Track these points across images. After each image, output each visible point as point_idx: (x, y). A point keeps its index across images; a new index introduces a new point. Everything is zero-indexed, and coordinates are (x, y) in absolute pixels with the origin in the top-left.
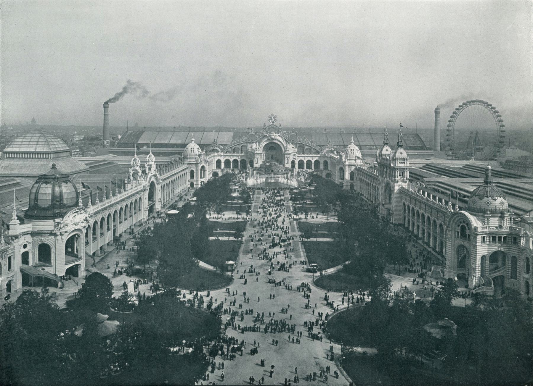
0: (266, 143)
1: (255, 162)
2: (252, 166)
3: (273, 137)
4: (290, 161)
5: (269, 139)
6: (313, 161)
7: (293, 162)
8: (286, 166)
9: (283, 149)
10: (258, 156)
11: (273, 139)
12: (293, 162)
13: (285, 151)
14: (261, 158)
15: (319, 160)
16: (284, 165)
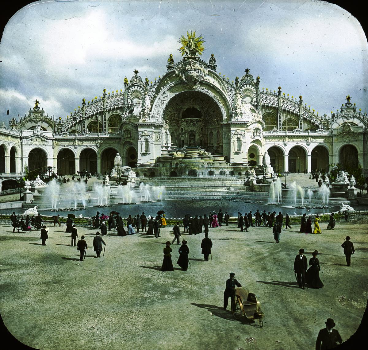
0: (170, 95)
1: (141, 148)
2: (131, 159)
3: (194, 74)
4: (247, 145)
5: (182, 83)
6: (309, 149)
7: (253, 153)
8: (235, 159)
9: (223, 111)
10: (147, 131)
11: (193, 81)
12: (253, 153)
13: (230, 116)
14: (158, 139)
15: (327, 146)
16: (227, 159)
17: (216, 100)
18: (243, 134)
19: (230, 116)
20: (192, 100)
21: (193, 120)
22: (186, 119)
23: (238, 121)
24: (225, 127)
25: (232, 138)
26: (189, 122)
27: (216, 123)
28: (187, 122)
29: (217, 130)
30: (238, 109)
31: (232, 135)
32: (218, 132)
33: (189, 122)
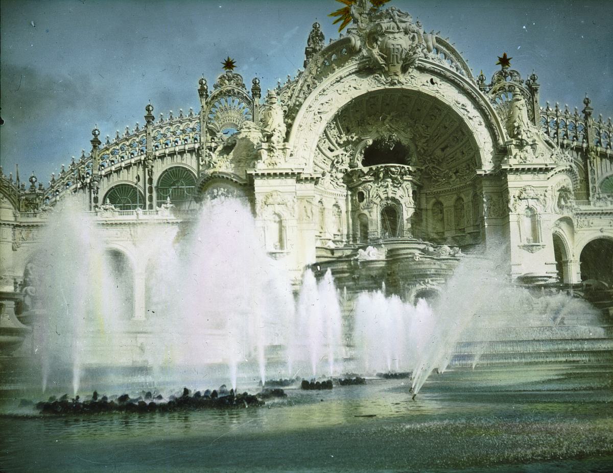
17: (461, 112)
18: (542, 198)
19: (501, 152)
20: (389, 118)
21: (393, 169)
22: (374, 167)
23: (528, 162)
24: (487, 183)
25: (513, 209)
26: (381, 175)
27: (451, 177)
28: (376, 175)
29: (455, 197)
30: (522, 132)
31: (512, 201)
32: (459, 199)
33: (381, 175)
